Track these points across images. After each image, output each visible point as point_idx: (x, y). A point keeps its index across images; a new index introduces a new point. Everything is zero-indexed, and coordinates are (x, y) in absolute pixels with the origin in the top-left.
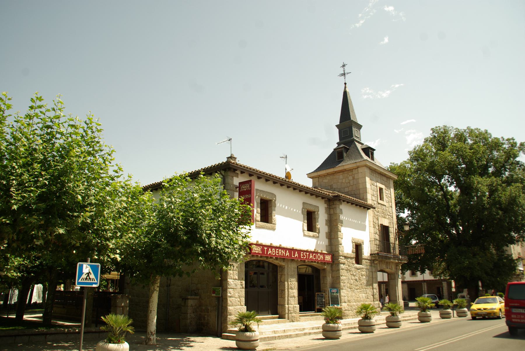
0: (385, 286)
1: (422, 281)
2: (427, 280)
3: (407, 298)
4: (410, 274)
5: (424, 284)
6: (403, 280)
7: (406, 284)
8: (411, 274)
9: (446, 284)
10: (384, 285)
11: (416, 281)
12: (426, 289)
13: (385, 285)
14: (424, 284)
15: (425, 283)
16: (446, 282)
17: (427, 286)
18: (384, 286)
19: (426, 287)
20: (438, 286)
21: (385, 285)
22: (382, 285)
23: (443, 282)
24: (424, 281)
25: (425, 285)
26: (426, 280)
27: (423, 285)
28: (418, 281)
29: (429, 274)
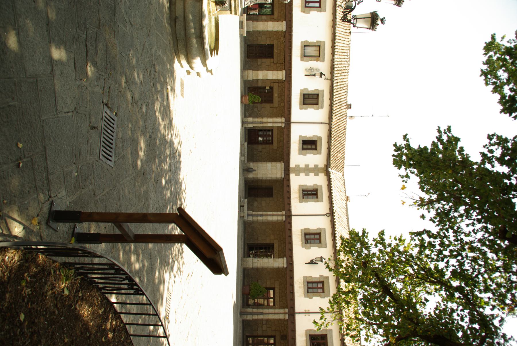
0: (281, 127)
1: (290, 210)
2: (290, 223)
3: (251, 176)
4: (306, 185)
5: (282, 215)
6: (291, 170)
7: (283, 176)
8: (305, 188)
9: (281, 265)
10: (282, 123)
11: (289, 198)
12: (270, 218)
13: (283, 125)
14: (282, 215)
15: (284, 218)
16: (285, 266)
17: (277, 223)
18: (280, 125)
19: (275, 218)
20: (276, 246)
21: (283, 125)
22: (283, 120)
23: (285, 259)
24: (289, 216)
25: (280, 218)
26: (291, 220)
27: (280, 213)
28: (289, 204)
29: (305, 229)
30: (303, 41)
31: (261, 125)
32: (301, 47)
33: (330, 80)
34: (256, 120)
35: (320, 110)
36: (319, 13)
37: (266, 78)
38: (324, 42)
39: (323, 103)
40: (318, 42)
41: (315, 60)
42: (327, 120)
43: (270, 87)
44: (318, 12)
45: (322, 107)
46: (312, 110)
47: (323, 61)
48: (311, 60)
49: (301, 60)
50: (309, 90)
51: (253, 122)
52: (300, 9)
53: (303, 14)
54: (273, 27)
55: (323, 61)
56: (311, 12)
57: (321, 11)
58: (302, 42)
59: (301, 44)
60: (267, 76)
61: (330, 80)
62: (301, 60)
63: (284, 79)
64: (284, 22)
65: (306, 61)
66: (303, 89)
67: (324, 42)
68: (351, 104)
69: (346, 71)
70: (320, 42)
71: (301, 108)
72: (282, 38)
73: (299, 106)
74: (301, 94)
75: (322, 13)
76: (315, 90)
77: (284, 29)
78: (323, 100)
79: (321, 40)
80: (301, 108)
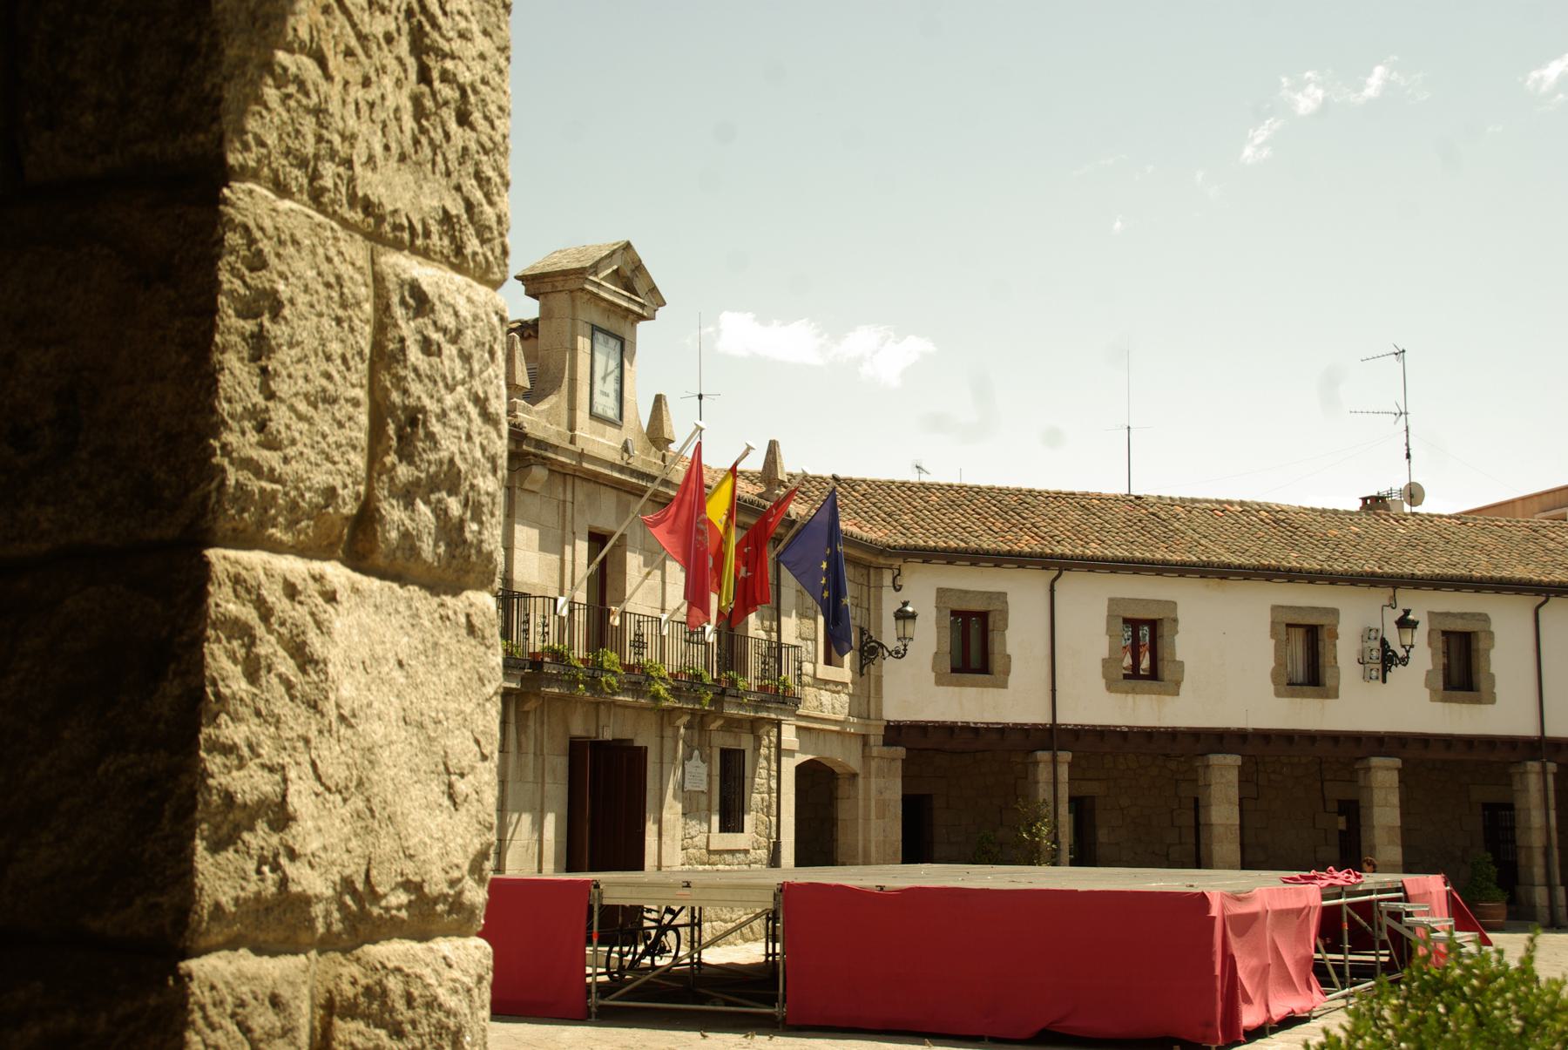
10: (1544, 772)
22: (1533, 766)
30: (1272, 687)
31: (1556, 853)
32: (1292, 696)
33: (1395, 588)
34: (1538, 872)
35: (1493, 628)
36: (1180, 627)
37: (1398, 832)
38: (1275, 609)
39: (1473, 615)
40: (1274, 634)
41: (1335, 645)
42: (1526, 603)
43: (1340, 813)
44: (1177, 632)
45: (1485, 618)
46: (1494, 654)
47: (1334, 612)
48: (1335, 658)
49: (1337, 697)
50: (1430, 667)
51: (1550, 886)
52: (1168, 698)
53: (1185, 687)
54: (1231, 803)
55: (1334, 612)
56: (1178, 658)
57: (1175, 620)
58: (1278, 694)
59: (1283, 697)
60: (1391, 828)
61: (1395, 588)
62: (1337, 697)
63: (1397, 762)
64: (1215, 759)
65: (1338, 678)
66: (1428, 691)
67: (1275, 609)
68: (1364, 500)
69: (1281, 521)
70: (1273, 623)
71: (1492, 699)
72: (1173, 765)
73: (1483, 706)
74: (1444, 700)
75: (1181, 614)
76: (1430, 644)
77: (1234, 760)
78: (1462, 616)
79: (1269, 620)
80: (1492, 699)
